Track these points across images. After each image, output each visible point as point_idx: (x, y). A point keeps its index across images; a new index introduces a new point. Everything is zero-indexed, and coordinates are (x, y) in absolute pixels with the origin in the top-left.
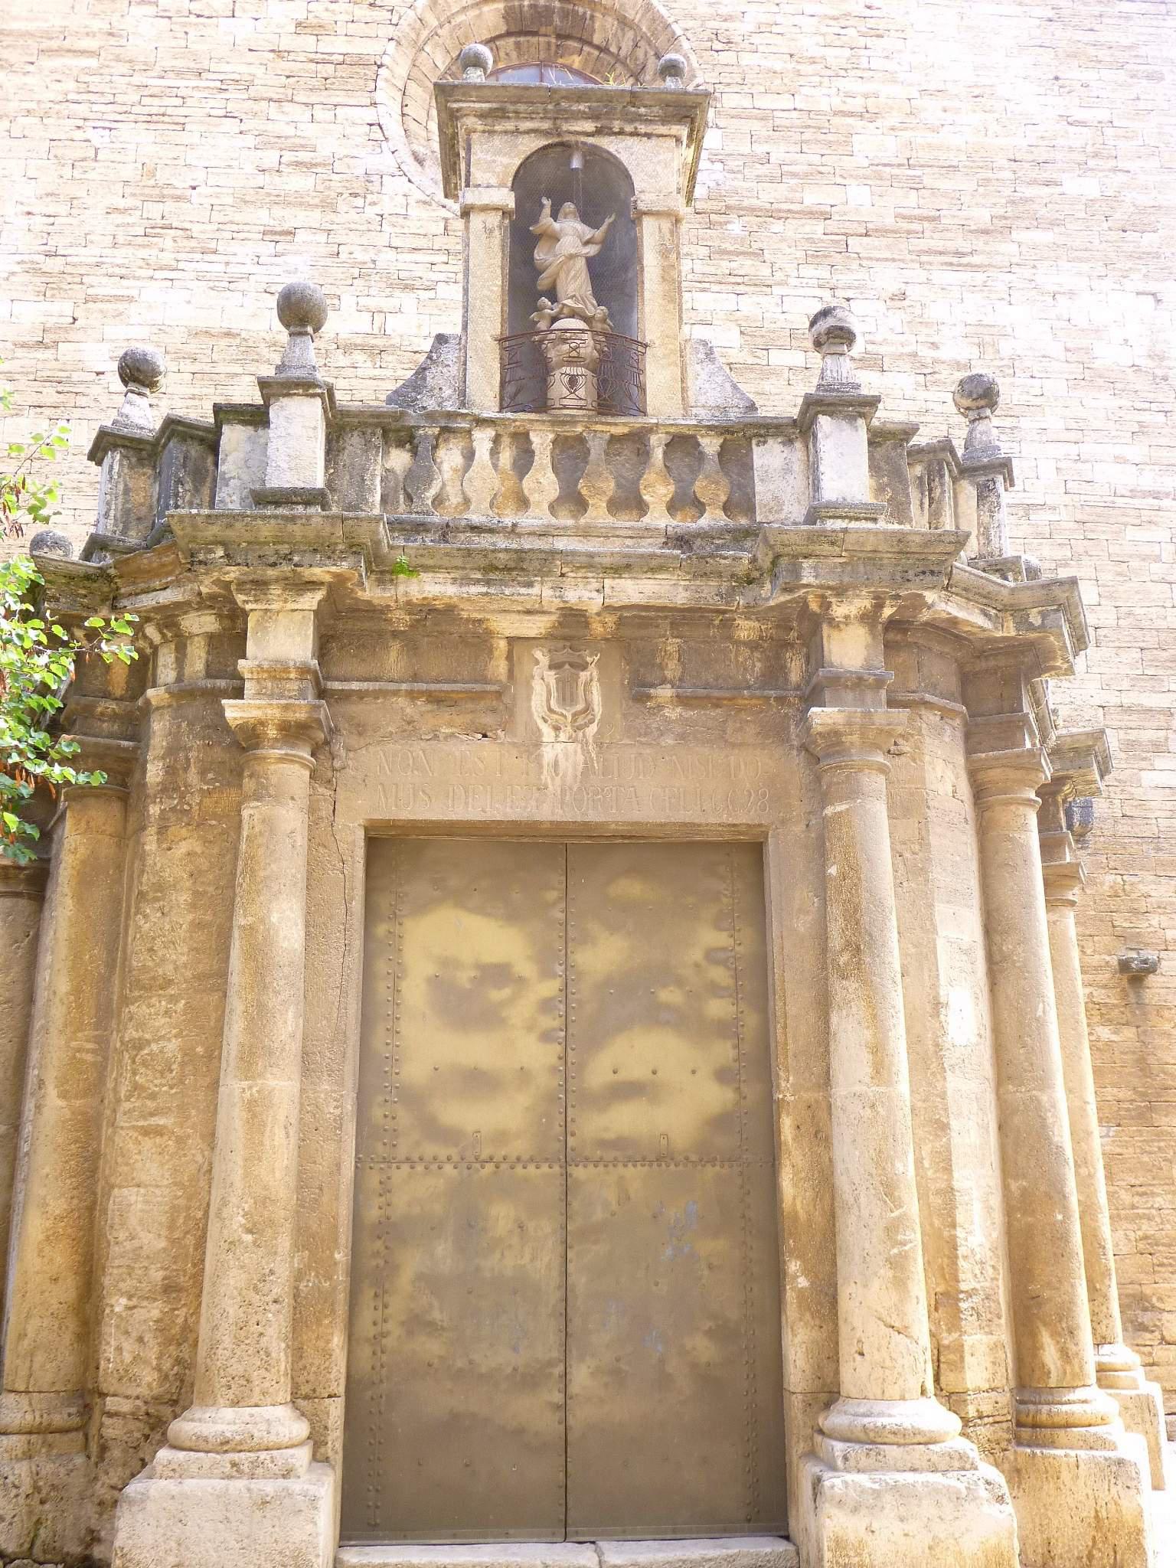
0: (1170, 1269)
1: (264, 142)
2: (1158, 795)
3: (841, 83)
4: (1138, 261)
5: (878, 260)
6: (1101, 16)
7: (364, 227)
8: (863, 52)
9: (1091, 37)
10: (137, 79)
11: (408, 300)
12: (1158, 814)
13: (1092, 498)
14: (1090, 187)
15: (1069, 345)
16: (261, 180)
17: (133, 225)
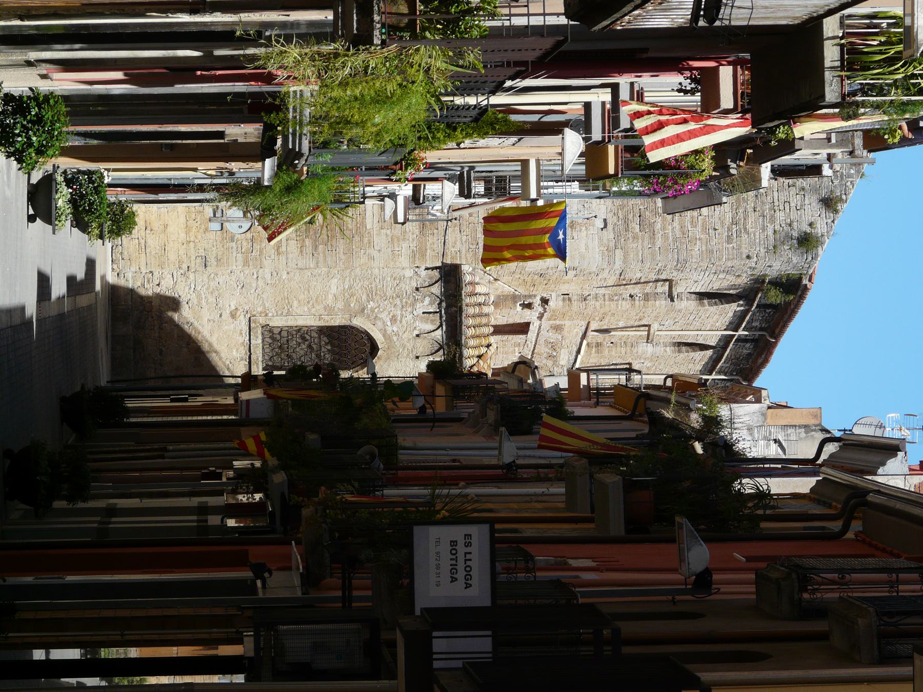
4: (623, 221)
6: (764, 216)
9: (750, 210)
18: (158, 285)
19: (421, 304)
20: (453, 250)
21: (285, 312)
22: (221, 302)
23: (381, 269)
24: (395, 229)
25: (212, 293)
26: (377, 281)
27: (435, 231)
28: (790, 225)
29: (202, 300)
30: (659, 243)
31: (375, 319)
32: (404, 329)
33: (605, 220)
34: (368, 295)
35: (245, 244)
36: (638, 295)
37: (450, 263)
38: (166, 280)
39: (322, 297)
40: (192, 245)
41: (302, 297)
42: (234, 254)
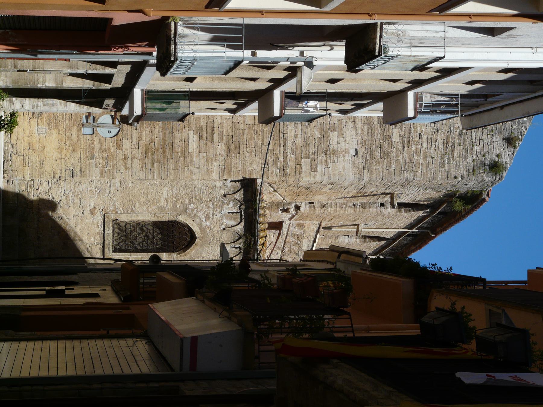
0: (49, 123)
2: (186, 135)
4: (369, 150)
6: (465, 149)
9: (456, 144)
12: (180, 134)
13: (282, 126)
15: (336, 124)
18: (38, 189)
19: (227, 207)
20: (250, 168)
21: (130, 210)
22: (84, 202)
23: (199, 181)
24: (209, 153)
25: (77, 196)
26: (196, 189)
27: (238, 155)
28: (484, 156)
29: (70, 200)
30: (394, 166)
31: (194, 216)
32: (215, 224)
33: (356, 150)
34: (190, 200)
35: (101, 161)
36: (359, 204)
37: (248, 177)
38: (44, 186)
39: (157, 200)
40: (63, 161)
41: (142, 200)
42: (94, 168)
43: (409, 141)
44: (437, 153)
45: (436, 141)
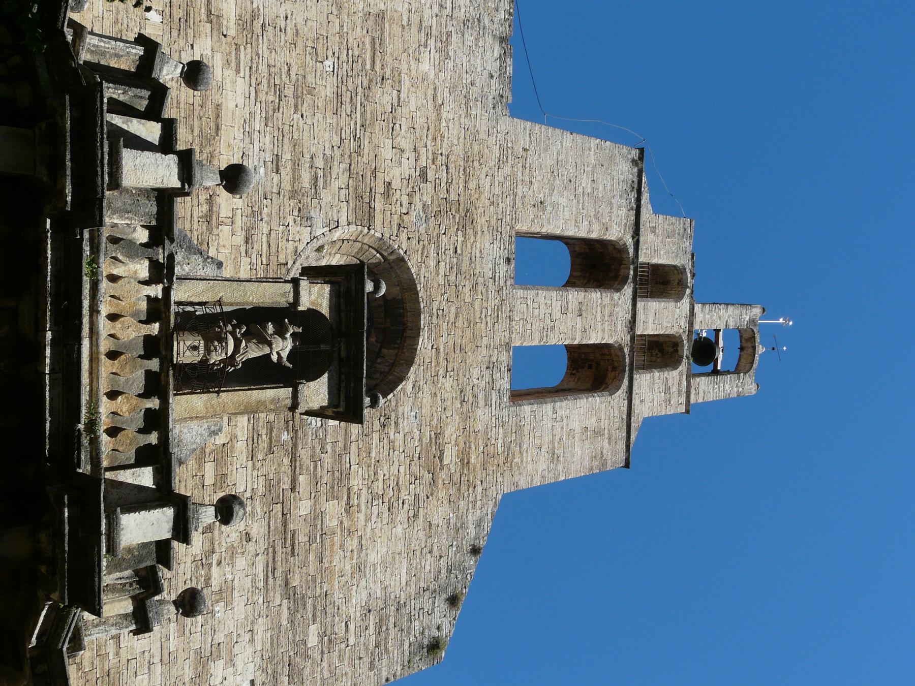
1: (328, 161)
3: (364, 491)
4: (272, 676)
5: (269, 522)
7: (281, 215)
8: (381, 501)
9: (391, 626)
10: (360, 90)
11: (239, 239)
14: (313, 640)
15: (222, 644)
16: (307, 156)
17: (281, 78)
43: (330, 641)
44: (367, 649)
45: (366, 629)
